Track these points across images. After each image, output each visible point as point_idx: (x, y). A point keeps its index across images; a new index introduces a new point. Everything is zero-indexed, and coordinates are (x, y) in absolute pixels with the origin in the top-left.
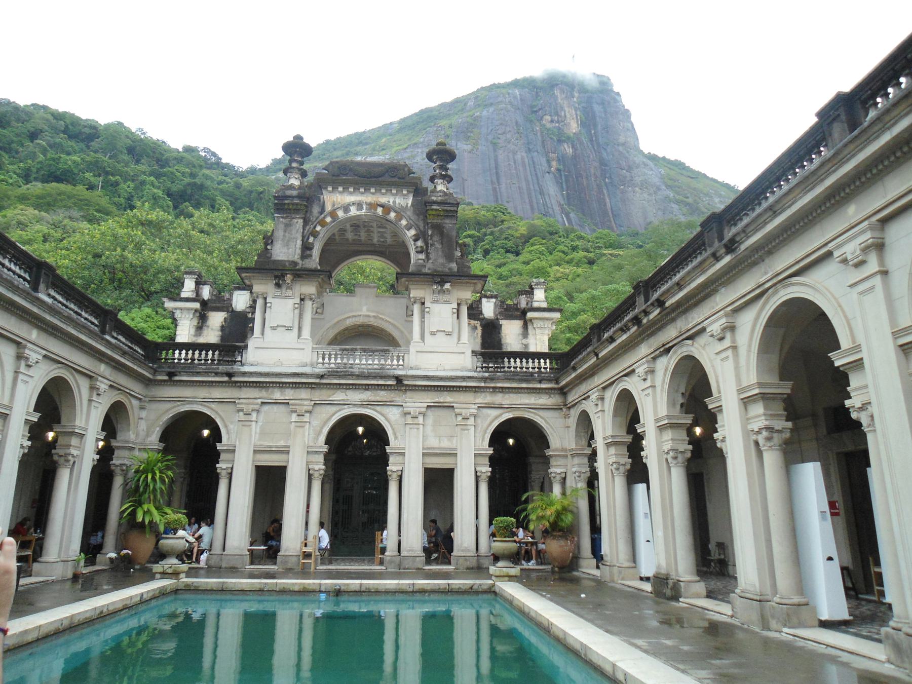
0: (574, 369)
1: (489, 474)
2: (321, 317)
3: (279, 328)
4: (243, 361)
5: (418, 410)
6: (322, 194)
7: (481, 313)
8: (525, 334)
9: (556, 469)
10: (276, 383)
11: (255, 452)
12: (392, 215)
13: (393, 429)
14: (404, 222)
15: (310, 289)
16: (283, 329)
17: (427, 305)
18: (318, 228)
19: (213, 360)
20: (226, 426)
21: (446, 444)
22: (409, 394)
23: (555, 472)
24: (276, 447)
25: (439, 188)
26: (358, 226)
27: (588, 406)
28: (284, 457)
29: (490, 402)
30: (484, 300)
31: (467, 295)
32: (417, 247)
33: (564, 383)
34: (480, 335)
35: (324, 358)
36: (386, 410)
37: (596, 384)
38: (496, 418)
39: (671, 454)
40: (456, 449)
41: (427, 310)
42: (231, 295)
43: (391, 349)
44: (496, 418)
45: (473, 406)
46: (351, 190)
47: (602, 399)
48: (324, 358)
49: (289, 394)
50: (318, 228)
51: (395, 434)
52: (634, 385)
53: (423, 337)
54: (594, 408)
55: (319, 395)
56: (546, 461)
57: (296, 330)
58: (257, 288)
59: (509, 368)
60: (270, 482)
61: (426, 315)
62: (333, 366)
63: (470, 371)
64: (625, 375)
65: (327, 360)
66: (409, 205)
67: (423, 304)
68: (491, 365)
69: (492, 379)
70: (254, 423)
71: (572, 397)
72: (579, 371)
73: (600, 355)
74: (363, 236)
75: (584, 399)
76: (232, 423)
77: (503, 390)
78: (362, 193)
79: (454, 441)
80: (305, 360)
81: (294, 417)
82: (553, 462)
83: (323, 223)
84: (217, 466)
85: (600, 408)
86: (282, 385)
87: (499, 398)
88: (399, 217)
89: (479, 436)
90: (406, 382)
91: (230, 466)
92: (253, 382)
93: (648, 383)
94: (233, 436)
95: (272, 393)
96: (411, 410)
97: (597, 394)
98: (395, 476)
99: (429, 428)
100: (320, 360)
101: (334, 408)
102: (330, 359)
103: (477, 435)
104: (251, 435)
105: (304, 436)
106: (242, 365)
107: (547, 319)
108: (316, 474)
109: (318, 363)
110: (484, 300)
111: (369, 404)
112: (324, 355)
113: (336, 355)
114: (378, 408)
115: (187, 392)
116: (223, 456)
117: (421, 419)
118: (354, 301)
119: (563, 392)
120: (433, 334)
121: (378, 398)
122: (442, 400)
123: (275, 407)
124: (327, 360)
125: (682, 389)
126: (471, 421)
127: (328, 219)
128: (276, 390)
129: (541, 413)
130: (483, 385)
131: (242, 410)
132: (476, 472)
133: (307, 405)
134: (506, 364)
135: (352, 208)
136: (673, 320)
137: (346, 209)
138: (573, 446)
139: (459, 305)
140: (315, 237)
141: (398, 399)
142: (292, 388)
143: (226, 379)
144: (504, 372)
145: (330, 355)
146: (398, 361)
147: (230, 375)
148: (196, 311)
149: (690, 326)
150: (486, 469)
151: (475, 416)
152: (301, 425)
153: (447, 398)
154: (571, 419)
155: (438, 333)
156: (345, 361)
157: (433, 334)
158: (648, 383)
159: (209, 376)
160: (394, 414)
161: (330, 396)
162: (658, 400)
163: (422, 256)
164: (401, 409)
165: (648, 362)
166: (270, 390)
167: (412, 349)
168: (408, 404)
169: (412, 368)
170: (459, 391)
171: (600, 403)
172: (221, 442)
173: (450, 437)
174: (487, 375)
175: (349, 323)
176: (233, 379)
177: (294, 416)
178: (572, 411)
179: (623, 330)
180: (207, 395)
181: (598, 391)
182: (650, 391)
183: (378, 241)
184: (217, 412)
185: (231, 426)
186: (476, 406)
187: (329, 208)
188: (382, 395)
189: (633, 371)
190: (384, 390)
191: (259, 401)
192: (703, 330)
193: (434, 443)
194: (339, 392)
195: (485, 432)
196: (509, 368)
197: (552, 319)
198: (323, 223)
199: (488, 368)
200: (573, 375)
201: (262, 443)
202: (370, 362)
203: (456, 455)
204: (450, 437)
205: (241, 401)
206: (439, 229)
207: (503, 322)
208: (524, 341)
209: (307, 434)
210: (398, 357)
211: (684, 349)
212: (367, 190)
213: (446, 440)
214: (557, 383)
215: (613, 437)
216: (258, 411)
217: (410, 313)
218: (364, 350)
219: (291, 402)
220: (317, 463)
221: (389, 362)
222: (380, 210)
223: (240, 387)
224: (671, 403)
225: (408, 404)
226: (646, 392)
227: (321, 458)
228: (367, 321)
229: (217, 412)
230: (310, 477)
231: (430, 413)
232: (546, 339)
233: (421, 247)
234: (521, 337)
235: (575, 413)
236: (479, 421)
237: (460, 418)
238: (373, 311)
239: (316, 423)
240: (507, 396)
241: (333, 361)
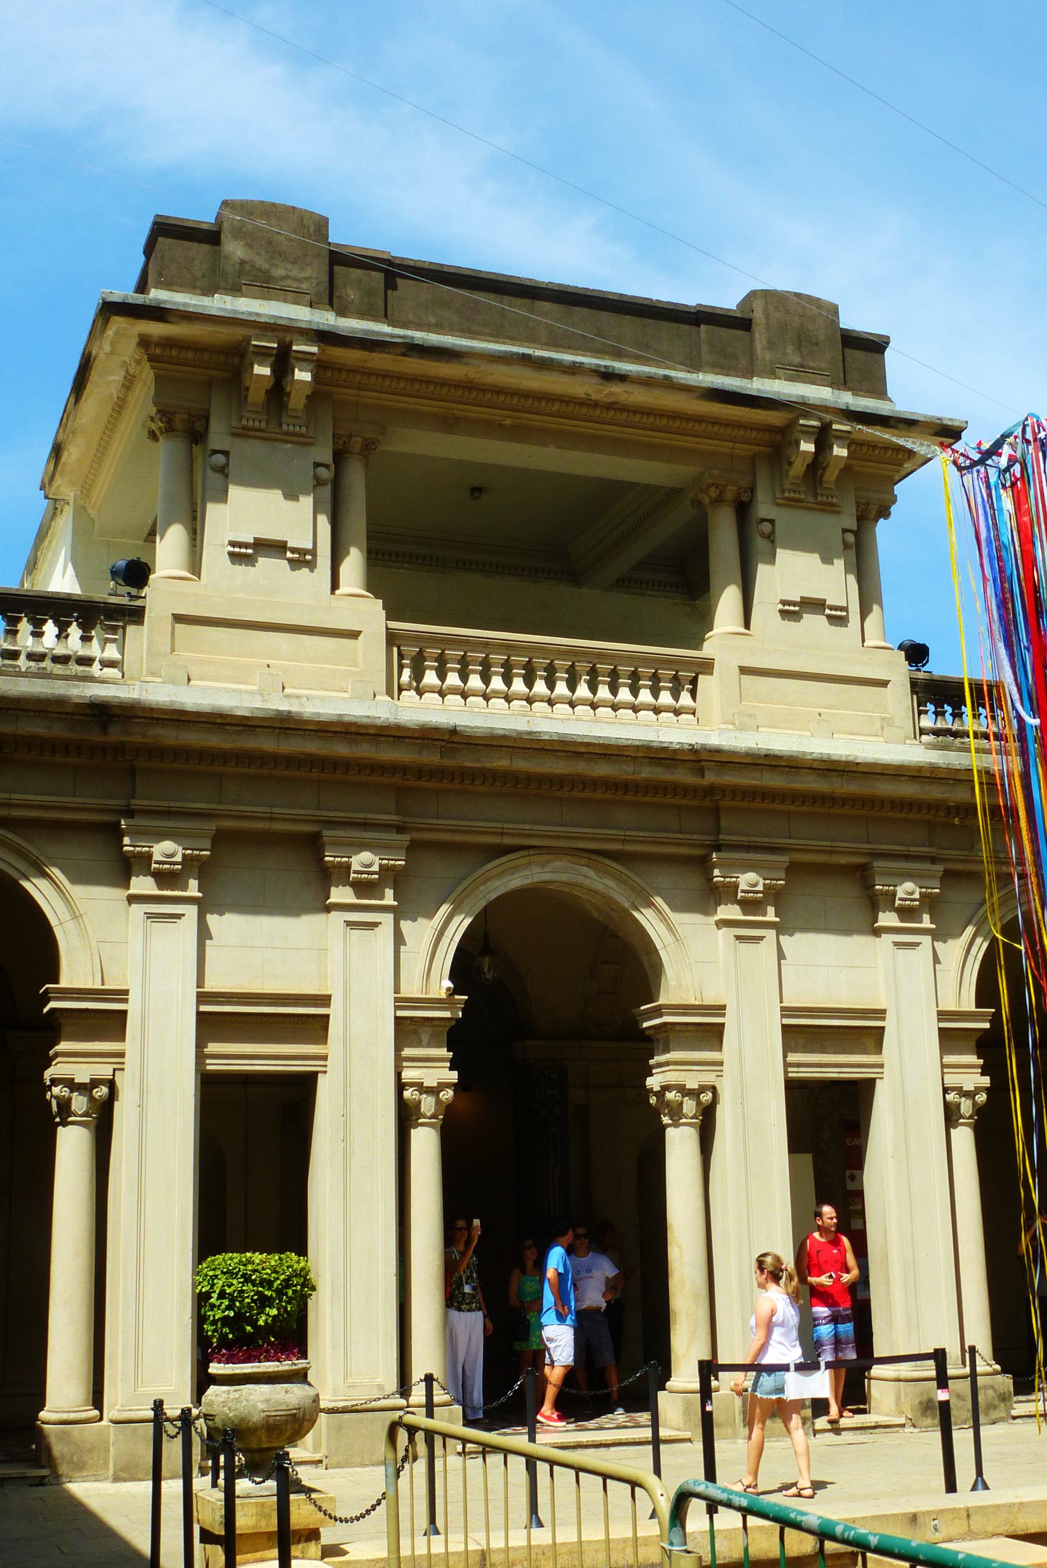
41: (766, 527)
108: (428, 1105)
230: (406, 1117)
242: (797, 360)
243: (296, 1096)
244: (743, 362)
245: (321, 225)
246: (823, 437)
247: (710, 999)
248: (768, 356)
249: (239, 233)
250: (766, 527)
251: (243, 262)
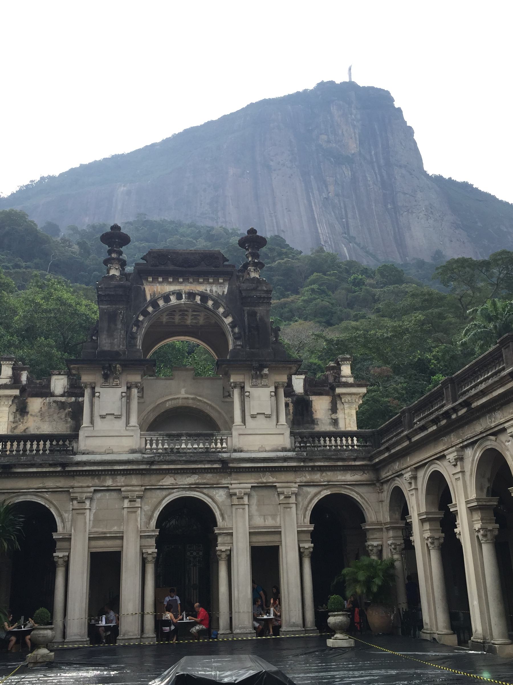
0: (388, 449)
1: (312, 550)
2: (142, 400)
3: (108, 417)
4: (75, 450)
5: (243, 491)
6: (143, 285)
7: (294, 391)
8: (334, 409)
9: (373, 543)
10: (108, 470)
11: (90, 539)
12: (210, 303)
13: (220, 510)
14: (221, 310)
15: (136, 378)
16: (113, 417)
18: (141, 318)
19: (44, 450)
20: (61, 516)
21: (270, 522)
22: (234, 476)
23: (372, 545)
24: (110, 533)
25: (253, 275)
26: (174, 311)
27: (403, 483)
28: (118, 542)
29: (309, 480)
30: (293, 376)
31: (284, 379)
32: (234, 334)
33: (377, 460)
34: (291, 411)
35: (151, 445)
36: (213, 492)
37: (409, 464)
38: (316, 495)
39: (482, 532)
40: (280, 527)
41: (247, 394)
42: (49, 381)
43: (215, 433)
44: (316, 495)
45: (294, 485)
46: (171, 280)
47: (415, 478)
48: (151, 445)
49: (121, 480)
50: (141, 318)
51: (222, 515)
52: (446, 469)
53: (244, 421)
54: (407, 485)
55: (148, 480)
56: (363, 535)
57: (124, 418)
58: (86, 378)
59: (326, 446)
60: (105, 568)
61: (246, 399)
62: (160, 451)
63: (289, 451)
64: (437, 459)
65: (154, 446)
66: (225, 293)
67: (242, 388)
68: (308, 445)
69: (311, 460)
70: (88, 511)
71: (385, 474)
72: (393, 451)
73: (414, 439)
74: (177, 319)
75: (398, 476)
76: (66, 512)
77: (321, 469)
78: (181, 283)
79: (278, 519)
80: (134, 447)
81: (126, 503)
82: (370, 536)
83: (145, 313)
84: (54, 554)
85: (413, 487)
86: (114, 473)
87: (317, 477)
88: (217, 305)
89: (301, 513)
90: (231, 465)
91: (67, 554)
92: (86, 471)
93: (458, 469)
94: (68, 525)
95: (105, 480)
96: (237, 491)
97: (410, 473)
98: (224, 555)
99: (254, 508)
100: (148, 446)
101: (165, 493)
102: (157, 445)
103: (299, 512)
104: (85, 523)
105: (136, 520)
106: (75, 454)
107: (354, 394)
108: (150, 558)
109: (146, 449)
110: (293, 376)
111: (196, 487)
112: (151, 441)
113: (163, 441)
114: (205, 491)
115: (21, 484)
116: (59, 545)
117: (246, 499)
118: (173, 383)
119: (376, 468)
120: (253, 417)
121: (205, 481)
122: (265, 481)
123: (107, 494)
124: (154, 446)
125: (488, 475)
126: (293, 500)
127: (150, 309)
128: (108, 477)
129: (357, 489)
130: (302, 464)
131: (76, 499)
132: (299, 548)
133: (138, 491)
134: (322, 442)
135: (172, 297)
136: (478, 418)
137: (166, 298)
138: (388, 520)
139: (276, 388)
140: (138, 327)
141: (224, 481)
142: (123, 475)
143: (59, 469)
144: (319, 451)
145: (157, 441)
146: (222, 444)
147: (64, 465)
148: (15, 397)
149: (493, 425)
150: (308, 545)
151: (296, 495)
152: (132, 510)
153: (268, 478)
154: (385, 493)
155: (258, 416)
156: (172, 446)
157: (253, 417)
158: (458, 469)
159: (43, 467)
160: (221, 496)
161: (159, 481)
162: (468, 482)
163: (239, 343)
164: (226, 490)
165: (457, 451)
166: (102, 478)
167: (235, 433)
168: (233, 486)
169: (235, 451)
170: (281, 471)
171: (413, 482)
172: (56, 531)
173: (274, 516)
174: (305, 454)
175: (168, 405)
176: (68, 469)
177: (126, 501)
178: (385, 487)
179: (435, 421)
180: (41, 485)
181: (411, 471)
182: (460, 475)
183: (191, 322)
184: (51, 502)
185: (66, 515)
186: (297, 485)
187: (148, 298)
188: (209, 478)
189: (444, 456)
190: (211, 473)
191: (92, 489)
192: (504, 430)
193: (259, 521)
194: (168, 476)
195: (306, 509)
196: (326, 446)
197: (359, 394)
198: (145, 313)
199: (307, 447)
200: (386, 455)
201: (95, 530)
202: (196, 446)
203: (280, 533)
204: (274, 516)
205: (76, 490)
206: (252, 314)
207: (313, 398)
208: (334, 416)
209: (139, 519)
210: (222, 440)
211: (488, 443)
212: (186, 280)
213: (270, 518)
214: (371, 459)
215: (427, 513)
216: (91, 499)
217: (227, 394)
218: (189, 435)
219: (123, 489)
220: (150, 547)
221: (213, 445)
222: (198, 299)
223: (73, 476)
224: (479, 487)
225: (233, 486)
226: (457, 476)
227: (153, 542)
228: (185, 403)
229: (51, 502)
230: (144, 562)
231: (254, 493)
232: (354, 412)
233: (239, 333)
234: (330, 412)
235: (388, 489)
236: (300, 499)
237: (282, 497)
238: (191, 394)
239: (146, 508)
240: (324, 474)
241: (160, 446)
250: (247, 394)
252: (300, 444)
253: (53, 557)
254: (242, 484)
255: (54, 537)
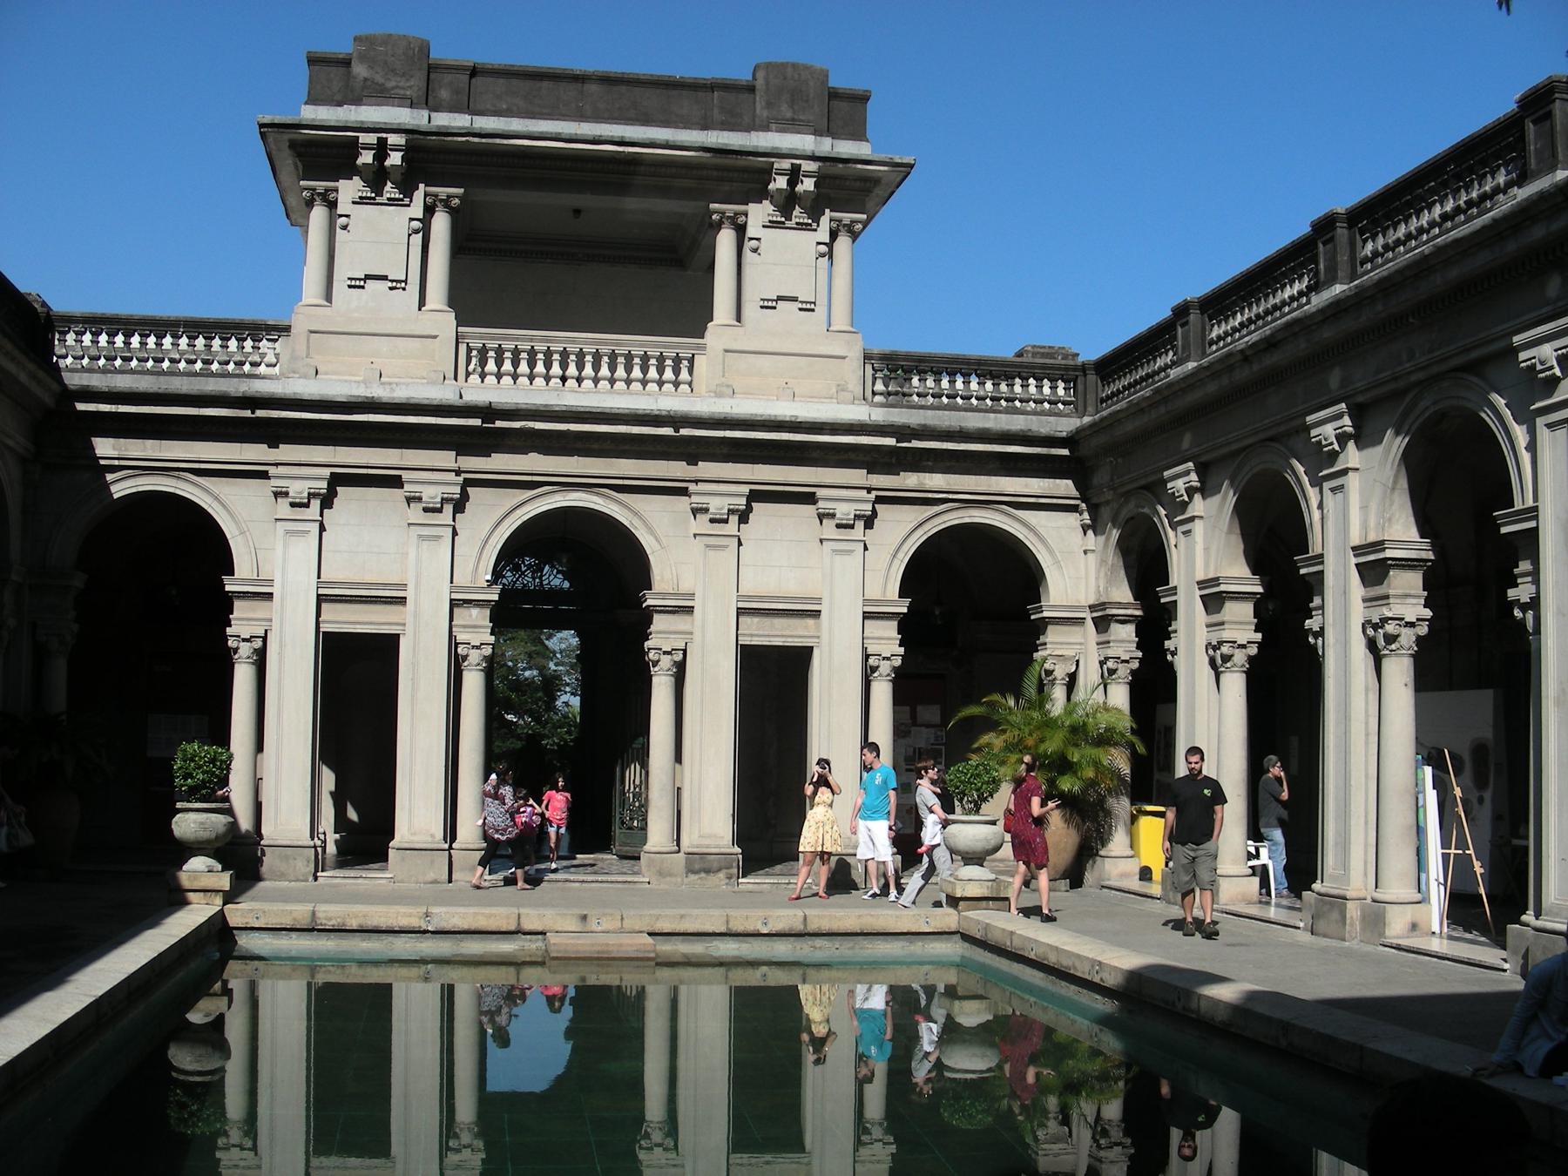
1: (898, 662)
17: (750, 232)
61: (748, 255)
84: (229, 630)
98: (666, 662)
120: (768, 306)
132: (867, 657)
242: (789, 115)
243: (386, 647)
244: (747, 119)
245: (425, 48)
246: (794, 175)
247: (685, 587)
248: (765, 113)
249: (363, 58)
251: (366, 79)
252: (886, 386)
253: (225, 638)
254: (723, 483)
255: (228, 588)
